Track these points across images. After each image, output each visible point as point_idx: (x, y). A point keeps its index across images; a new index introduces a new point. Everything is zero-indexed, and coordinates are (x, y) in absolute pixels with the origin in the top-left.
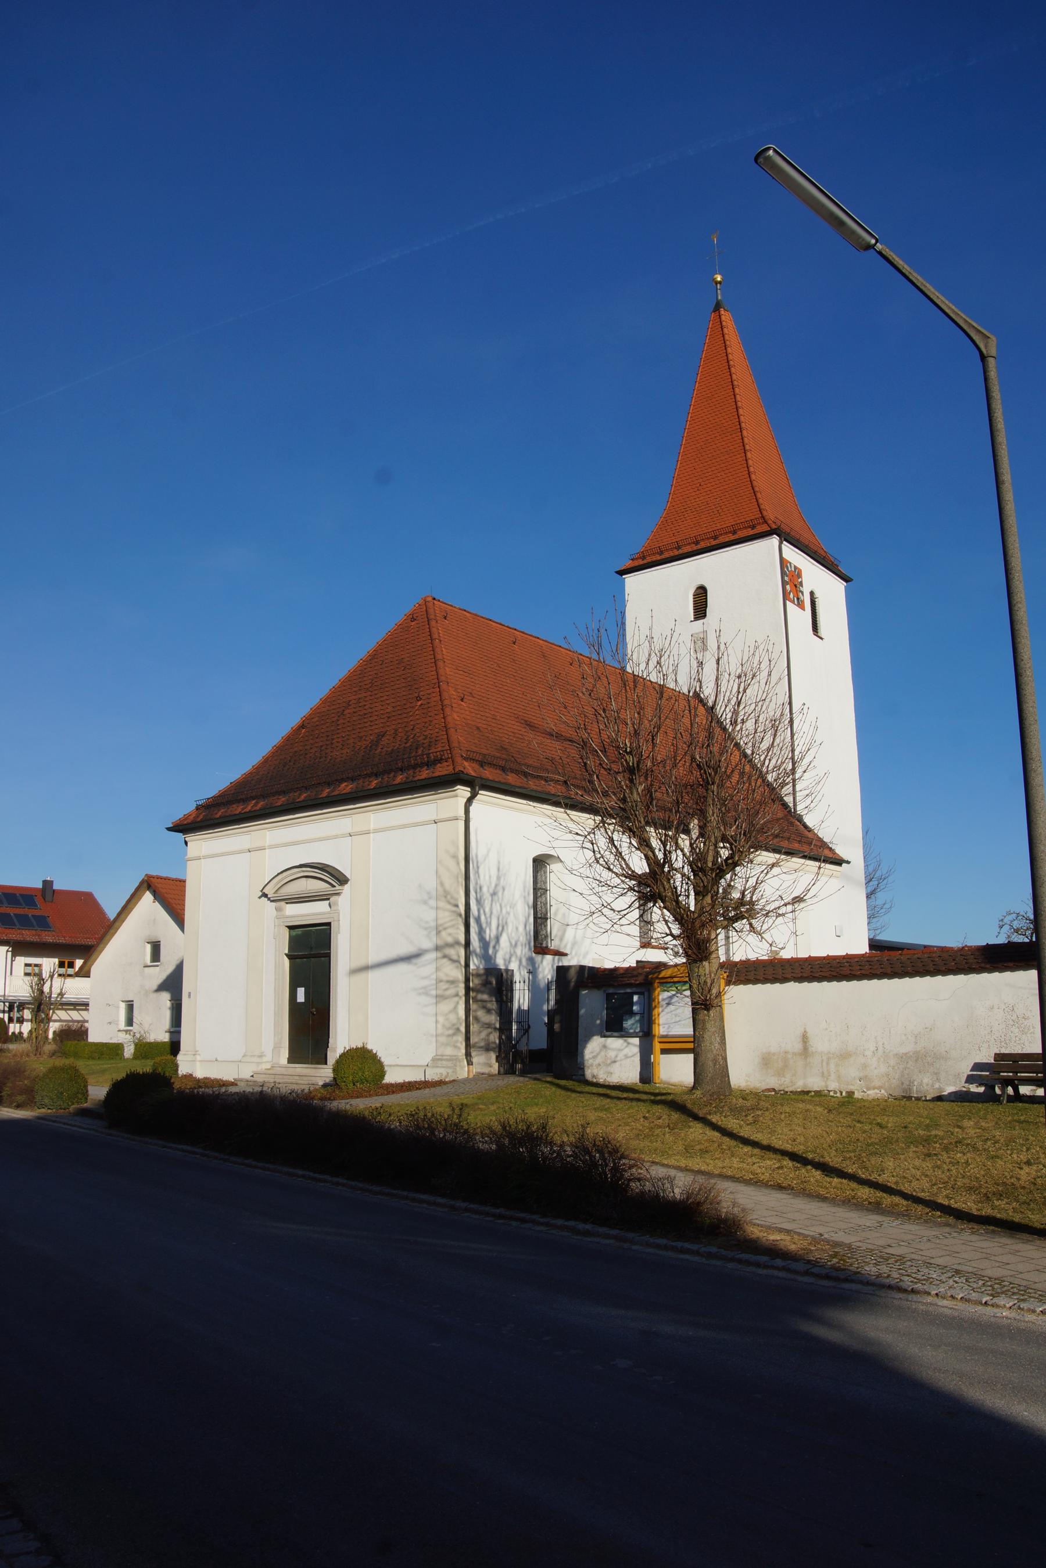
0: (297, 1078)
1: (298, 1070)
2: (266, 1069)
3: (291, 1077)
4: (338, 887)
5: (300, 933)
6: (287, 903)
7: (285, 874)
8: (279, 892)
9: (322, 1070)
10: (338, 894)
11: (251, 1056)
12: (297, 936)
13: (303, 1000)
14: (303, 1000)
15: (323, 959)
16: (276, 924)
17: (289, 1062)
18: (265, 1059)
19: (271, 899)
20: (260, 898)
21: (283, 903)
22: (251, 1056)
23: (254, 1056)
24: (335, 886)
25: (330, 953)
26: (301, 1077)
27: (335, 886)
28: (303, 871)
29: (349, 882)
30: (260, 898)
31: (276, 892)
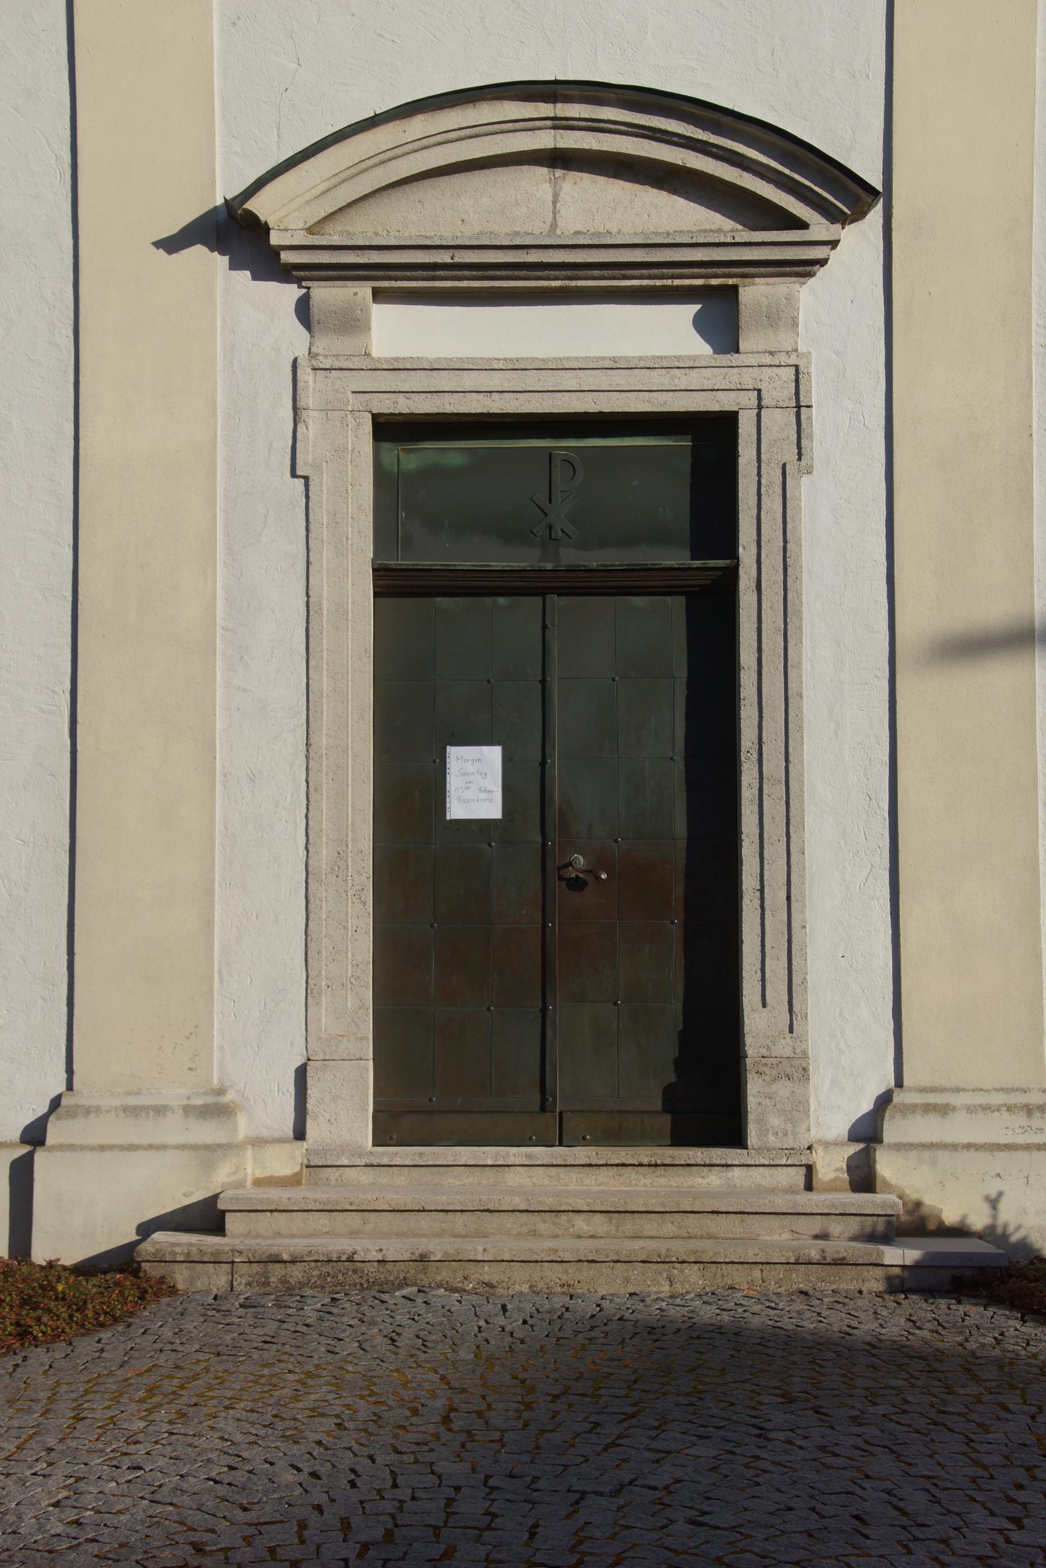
0: (599, 1224)
1: (514, 1178)
2: (258, 1182)
3: (543, 1225)
4: (820, 228)
5: (456, 460)
6: (378, 295)
7: (419, 126)
8: (329, 228)
9: (713, 1180)
10: (804, 269)
11: (134, 1111)
12: (427, 475)
13: (492, 809)
14: (492, 809)
15: (639, 601)
16: (309, 399)
17: (379, 1140)
18: (243, 1127)
19: (287, 257)
20: (172, 244)
21: (365, 290)
22: (134, 1111)
23: (160, 1110)
24: (803, 225)
25: (732, 574)
26: (629, 1225)
27: (803, 225)
28: (560, 124)
29: (876, 215)
30: (172, 244)
31: (310, 231)
